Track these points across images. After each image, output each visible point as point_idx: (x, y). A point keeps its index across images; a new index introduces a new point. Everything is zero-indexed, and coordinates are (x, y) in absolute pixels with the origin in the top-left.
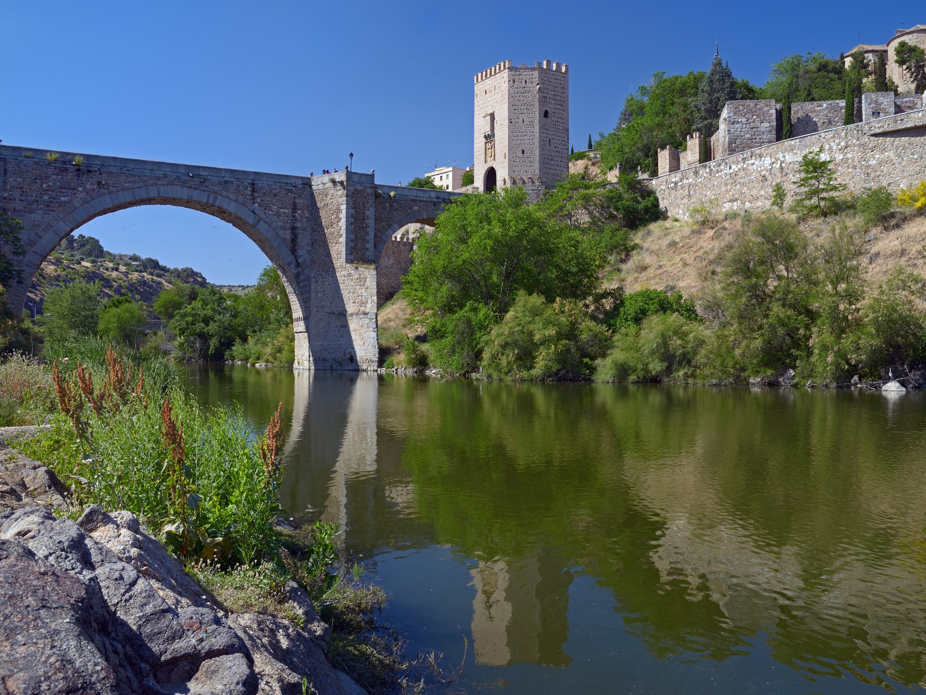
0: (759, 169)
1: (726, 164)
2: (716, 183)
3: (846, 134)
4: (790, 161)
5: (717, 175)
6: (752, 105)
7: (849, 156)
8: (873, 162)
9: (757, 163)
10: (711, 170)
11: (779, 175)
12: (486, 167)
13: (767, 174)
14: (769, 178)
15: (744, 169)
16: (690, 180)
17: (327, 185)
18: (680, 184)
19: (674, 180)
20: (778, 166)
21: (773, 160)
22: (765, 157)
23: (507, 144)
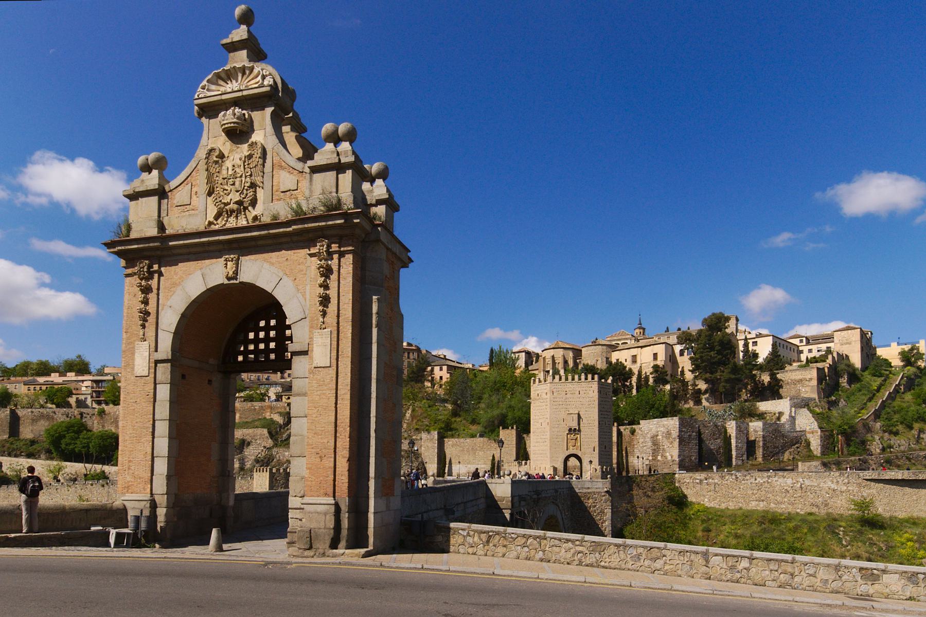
2: (742, 487)
5: (743, 482)
7: (849, 488)
8: (865, 494)
9: (780, 480)
10: (737, 478)
11: (800, 491)
12: (568, 453)
13: (789, 489)
15: (768, 483)
16: (716, 481)
21: (794, 481)
23: (597, 440)
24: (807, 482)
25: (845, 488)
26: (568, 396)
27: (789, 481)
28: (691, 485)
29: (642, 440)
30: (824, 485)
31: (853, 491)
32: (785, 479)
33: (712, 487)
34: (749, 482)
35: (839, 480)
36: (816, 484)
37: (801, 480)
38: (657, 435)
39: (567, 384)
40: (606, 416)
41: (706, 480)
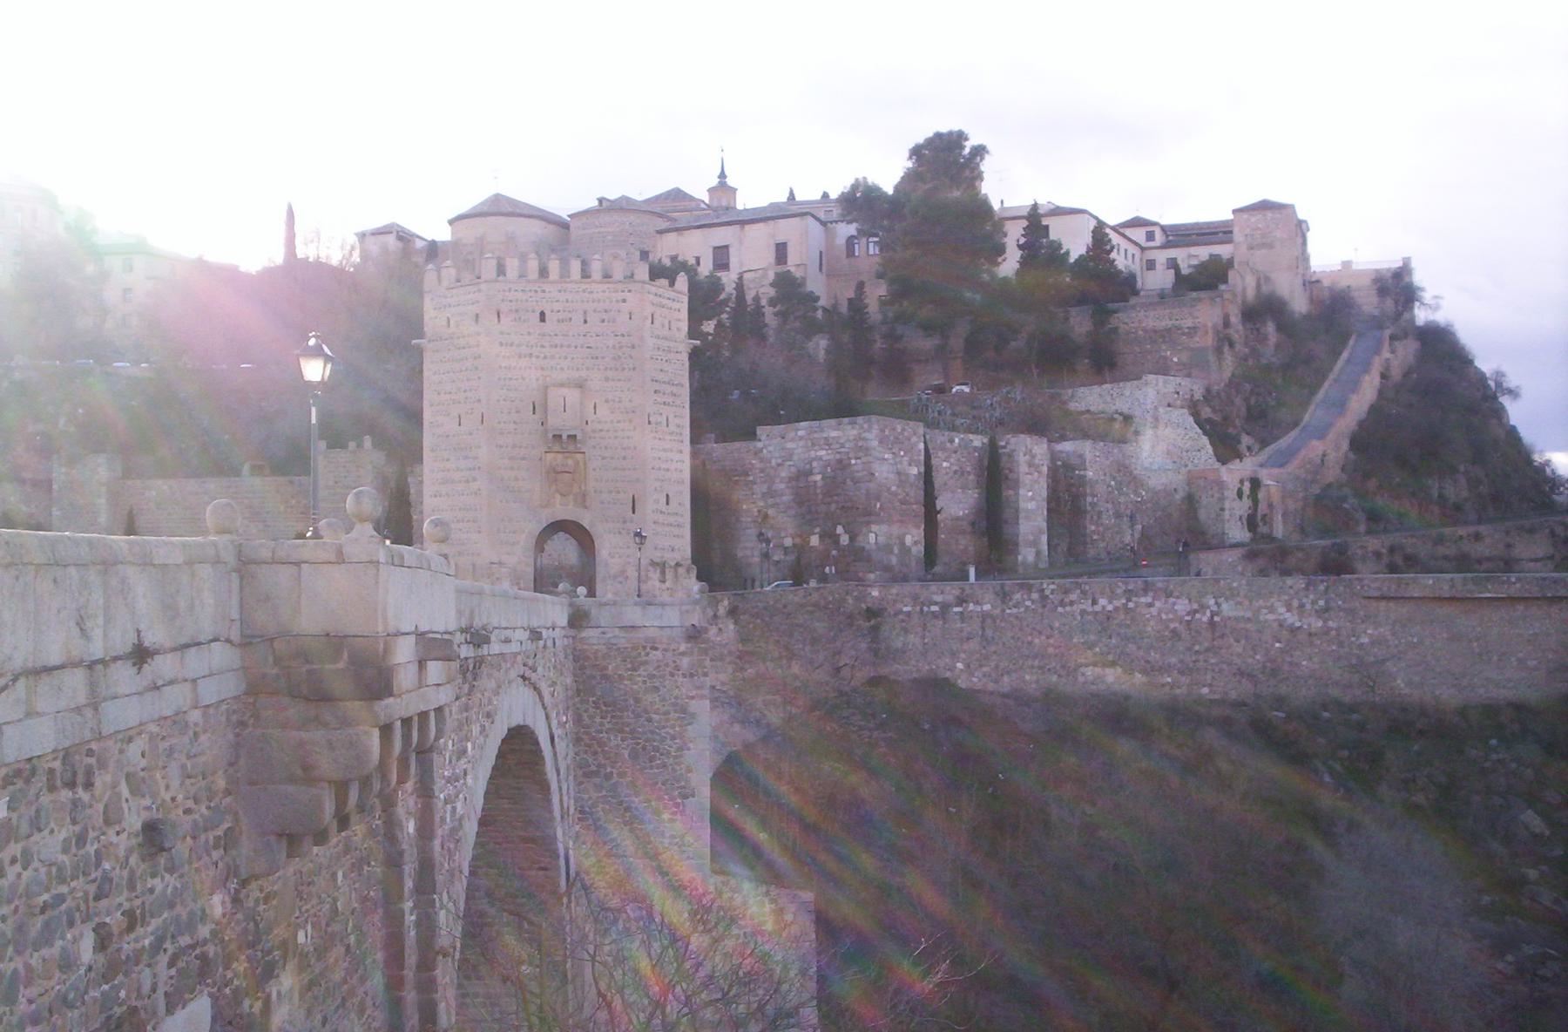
0: (1164, 617)
1: (1084, 593)
2: (1057, 625)
3: (1327, 588)
4: (1231, 614)
5: (1060, 609)
6: (899, 429)
7: (1331, 624)
9: (1158, 604)
10: (1044, 598)
12: (546, 517)
13: (1181, 628)
14: (1185, 634)
15: (1127, 610)
16: (987, 607)
17: (640, 634)
18: (957, 609)
19: (939, 598)
20: (1205, 619)
21: (1195, 606)
22: (1178, 597)
24: (1227, 609)
25: (1320, 624)
26: (549, 326)
27: (1182, 606)
28: (916, 620)
29: (764, 488)
30: (1270, 617)
31: (1338, 629)
32: (1172, 600)
33: (975, 626)
34: (1077, 608)
35: (1305, 600)
36: (1249, 614)
37: (1212, 602)
38: (810, 473)
39: (547, 287)
40: (670, 400)
41: (961, 601)
